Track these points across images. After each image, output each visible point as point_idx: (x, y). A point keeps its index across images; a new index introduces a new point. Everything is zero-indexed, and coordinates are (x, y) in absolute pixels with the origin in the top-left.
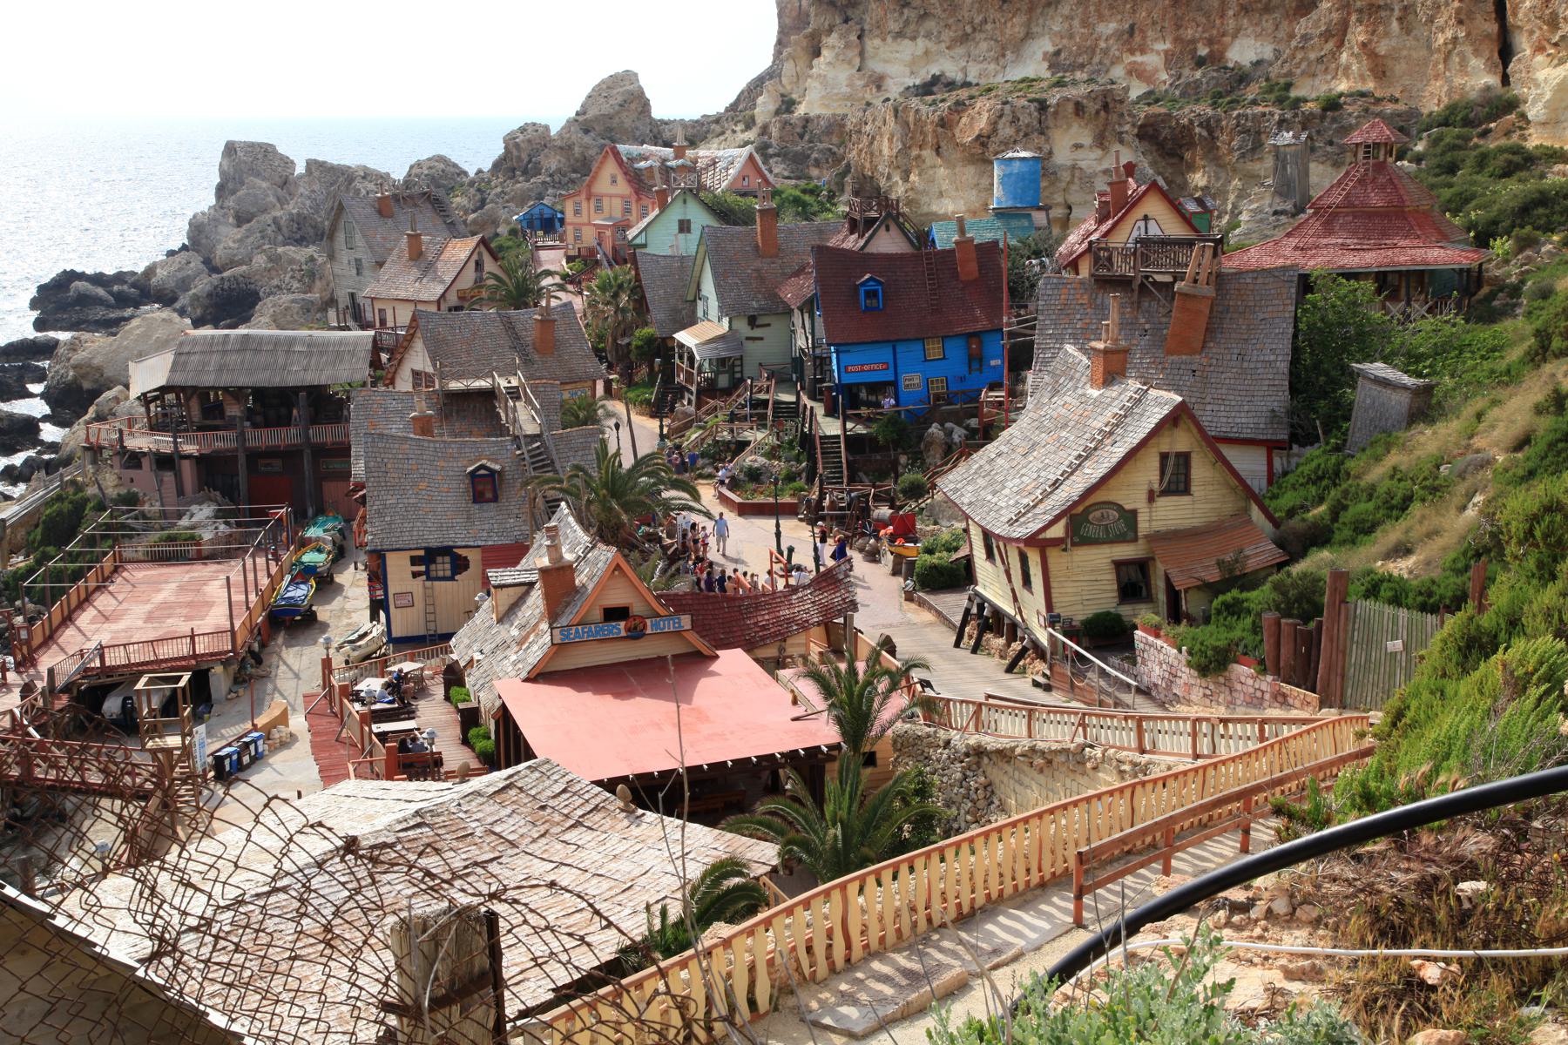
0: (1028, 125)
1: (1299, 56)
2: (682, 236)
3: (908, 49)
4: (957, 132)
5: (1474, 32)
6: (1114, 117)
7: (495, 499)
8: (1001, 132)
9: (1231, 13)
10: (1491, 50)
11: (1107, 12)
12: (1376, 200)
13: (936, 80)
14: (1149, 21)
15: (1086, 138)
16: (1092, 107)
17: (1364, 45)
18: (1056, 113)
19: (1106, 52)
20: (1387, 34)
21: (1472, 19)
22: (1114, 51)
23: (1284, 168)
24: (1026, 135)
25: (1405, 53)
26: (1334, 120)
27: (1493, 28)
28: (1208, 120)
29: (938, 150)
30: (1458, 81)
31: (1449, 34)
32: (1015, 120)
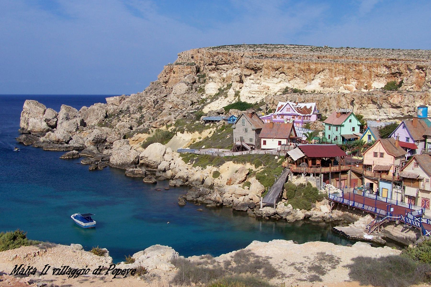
0: (411, 100)
3: (276, 80)
8: (405, 101)
9: (373, 77)
11: (337, 75)
13: (287, 88)
19: (338, 83)
22: (340, 83)
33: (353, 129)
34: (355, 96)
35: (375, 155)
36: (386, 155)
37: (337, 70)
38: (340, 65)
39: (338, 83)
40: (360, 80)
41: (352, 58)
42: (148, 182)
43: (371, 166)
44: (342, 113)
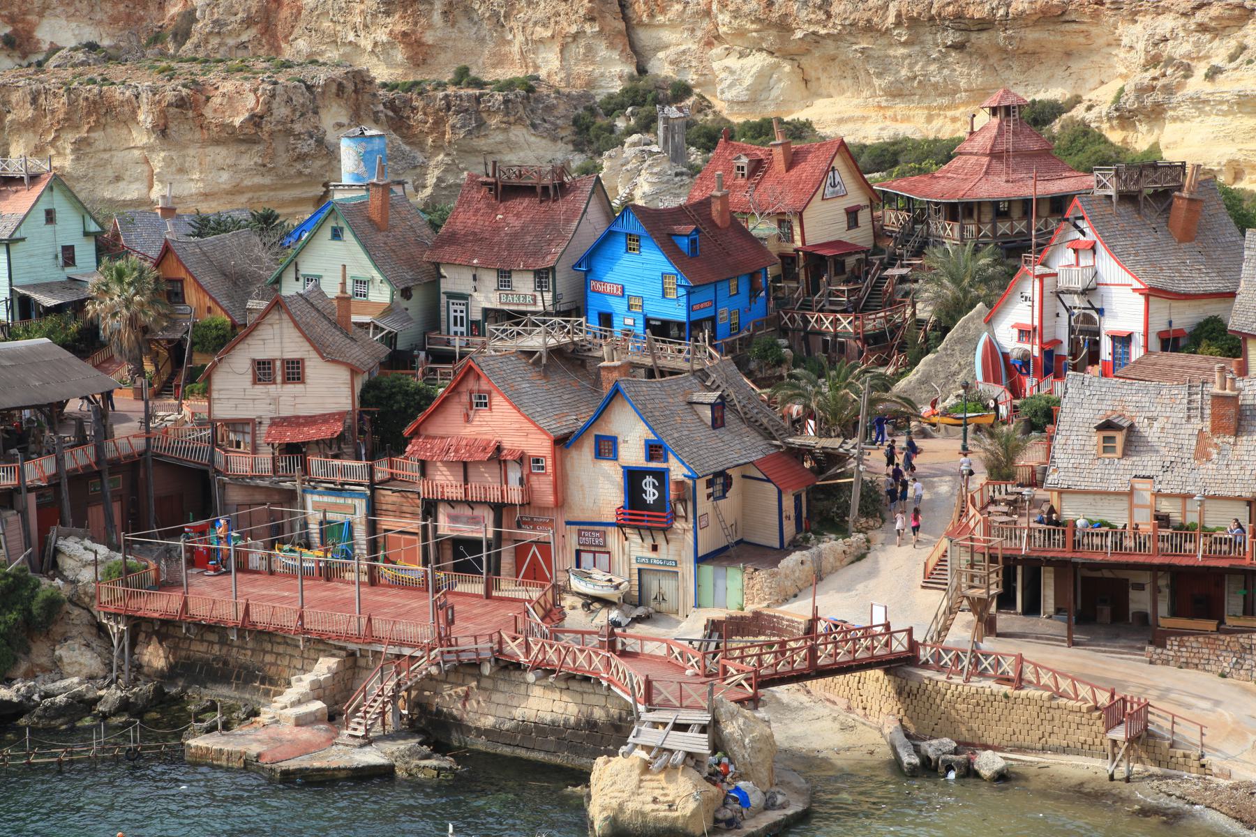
0: (303, 105)
1: (214, 41)
2: (49, 227)
4: (208, 112)
5: (607, 28)
6: (367, 98)
7: (723, 425)
10: (621, 42)
12: (1034, 145)
15: (345, 120)
16: (350, 87)
17: (405, 34)
18: (323, 93)
20: (430, 26)
21: (604, 18)
23: (673, 138)
24: (302, 115)
25: (450, 43)
26: (537, 100)
27: (621, 25)
28: (392, 101)
29: (162, 130)
30: (581, 69)
31: (574, 29)
32: (289, 100)
33: (68, 256)
36: (316, 369)
42: (522, 753)
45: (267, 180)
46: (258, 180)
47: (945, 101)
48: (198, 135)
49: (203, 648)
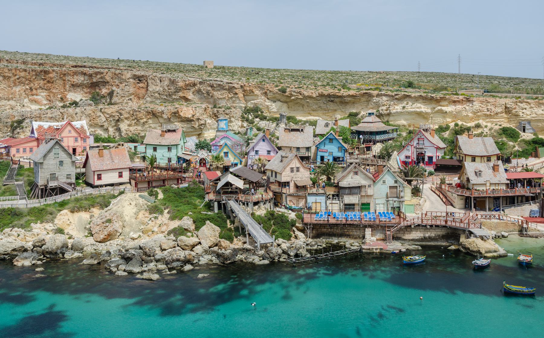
14: (39, 87)
34: (123, 110)
35: (292, 170)
36: (301, 169)
37: (17, 77)
38: (21, 71)
39: (20, 95)
40: (51, 90)
41: (16, 62)
43: (288, 183)
44: (167, 131)
45: (192, 130)
46: (191, 130)
47: (327, 112)
48: (178, 120)
49: (325, 230)
